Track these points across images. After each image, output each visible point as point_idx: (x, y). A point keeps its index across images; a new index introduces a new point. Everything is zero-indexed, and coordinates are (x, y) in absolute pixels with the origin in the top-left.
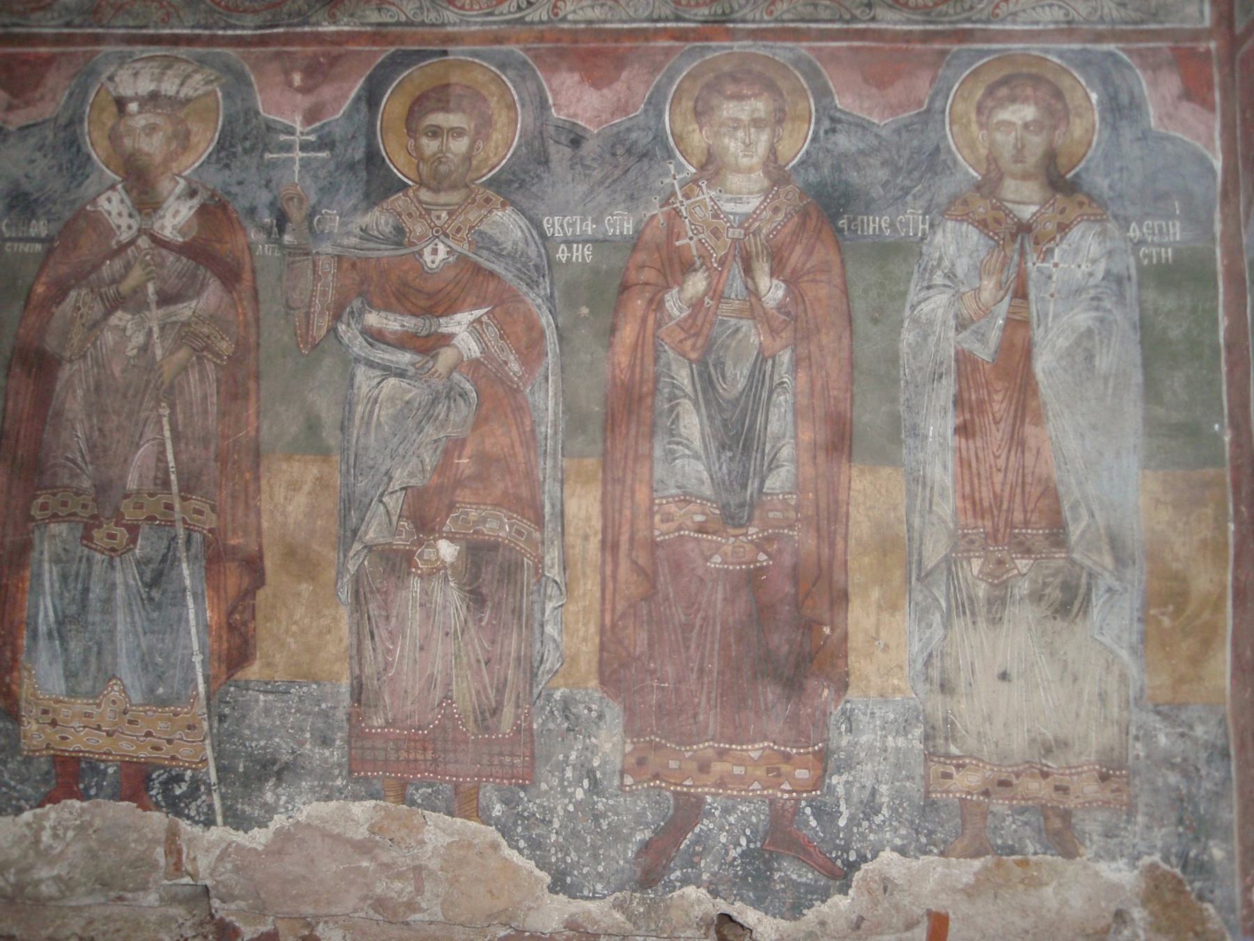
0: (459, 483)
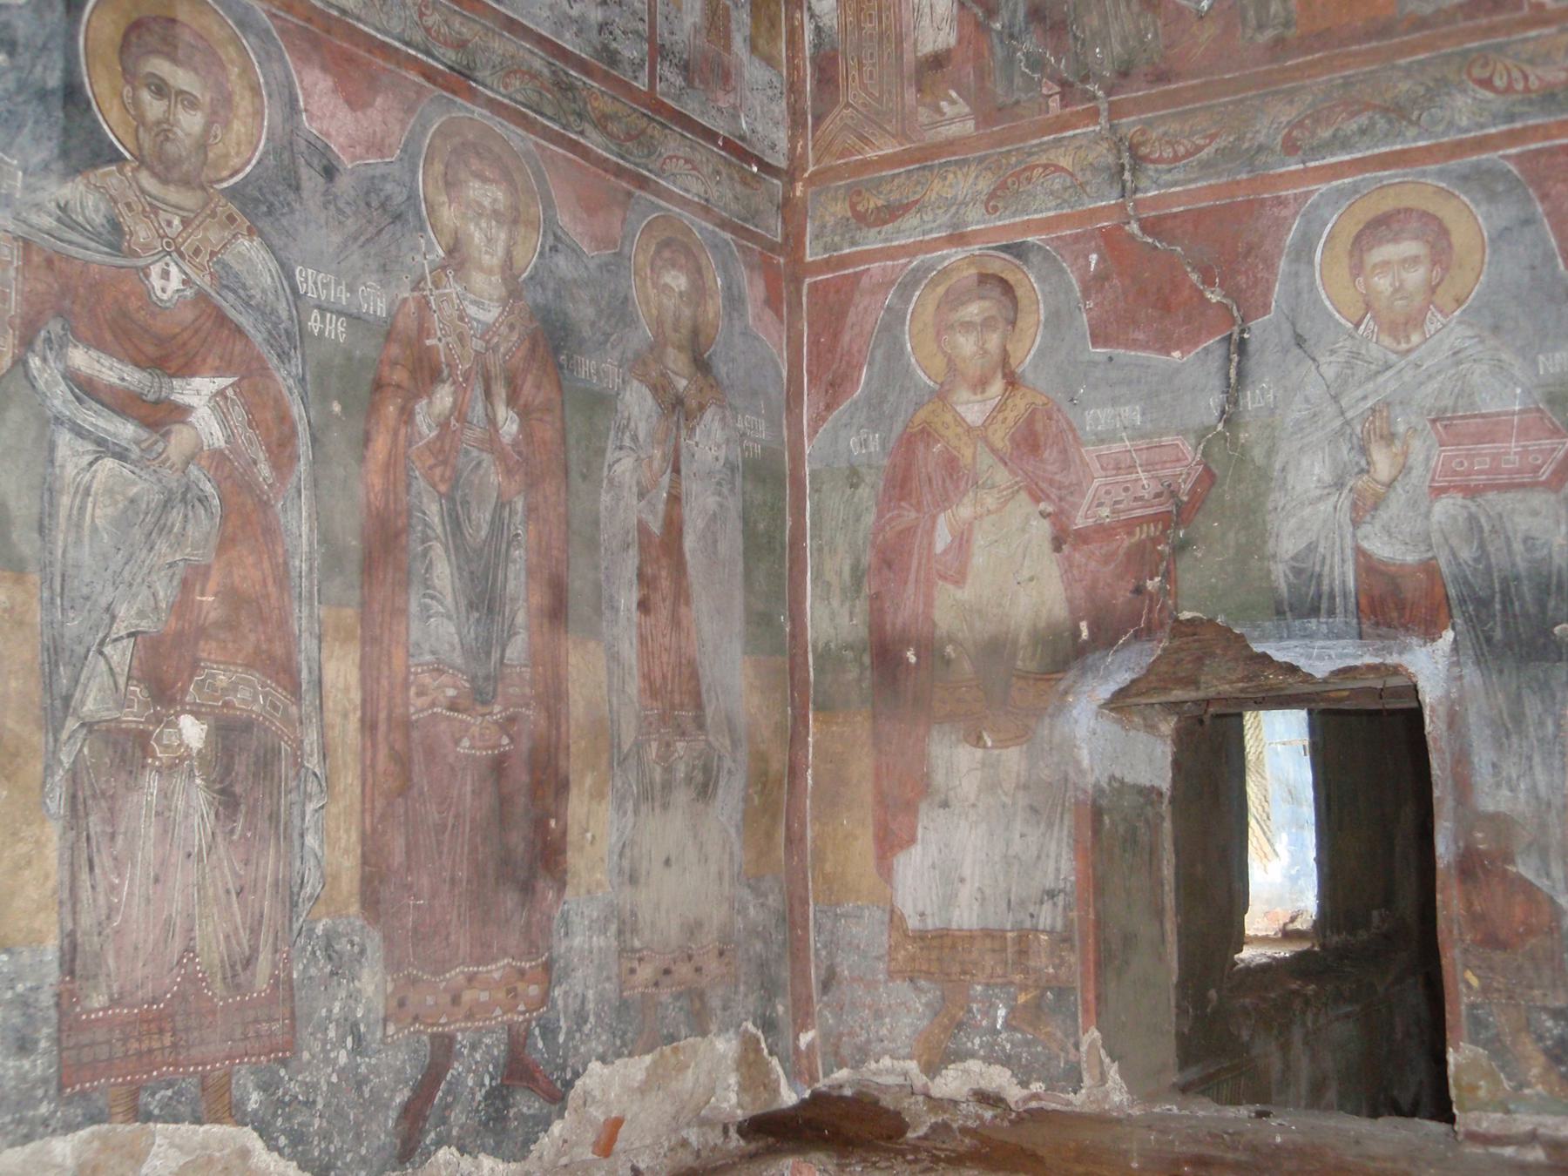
0: (202, 632)
